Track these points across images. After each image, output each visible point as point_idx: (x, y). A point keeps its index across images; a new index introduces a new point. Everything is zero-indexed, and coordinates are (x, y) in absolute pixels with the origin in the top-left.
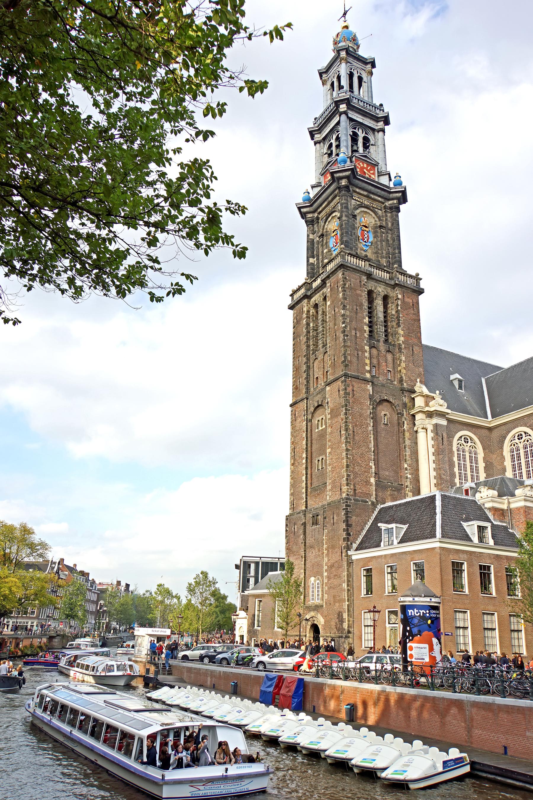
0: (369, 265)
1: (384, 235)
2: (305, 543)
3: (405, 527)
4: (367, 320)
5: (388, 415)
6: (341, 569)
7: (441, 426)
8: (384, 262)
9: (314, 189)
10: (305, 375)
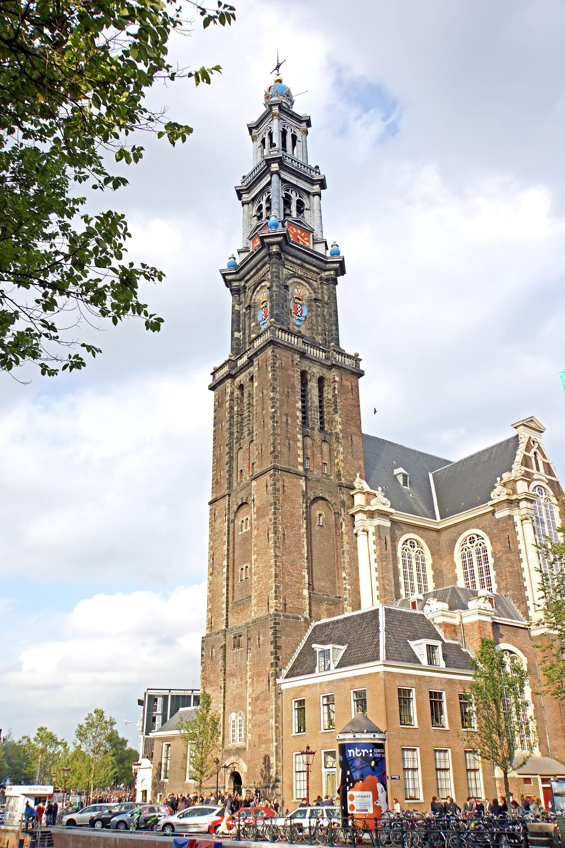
0: (303, 342)
1: (319, 309)
2: (225, 670)
3: (344, 648)
4: (299, 405)
5: (324, 515)
6: (267, 702)
7: (384, 527)
8: (319, 339)
9: (240, 254)
10: (227, 468)
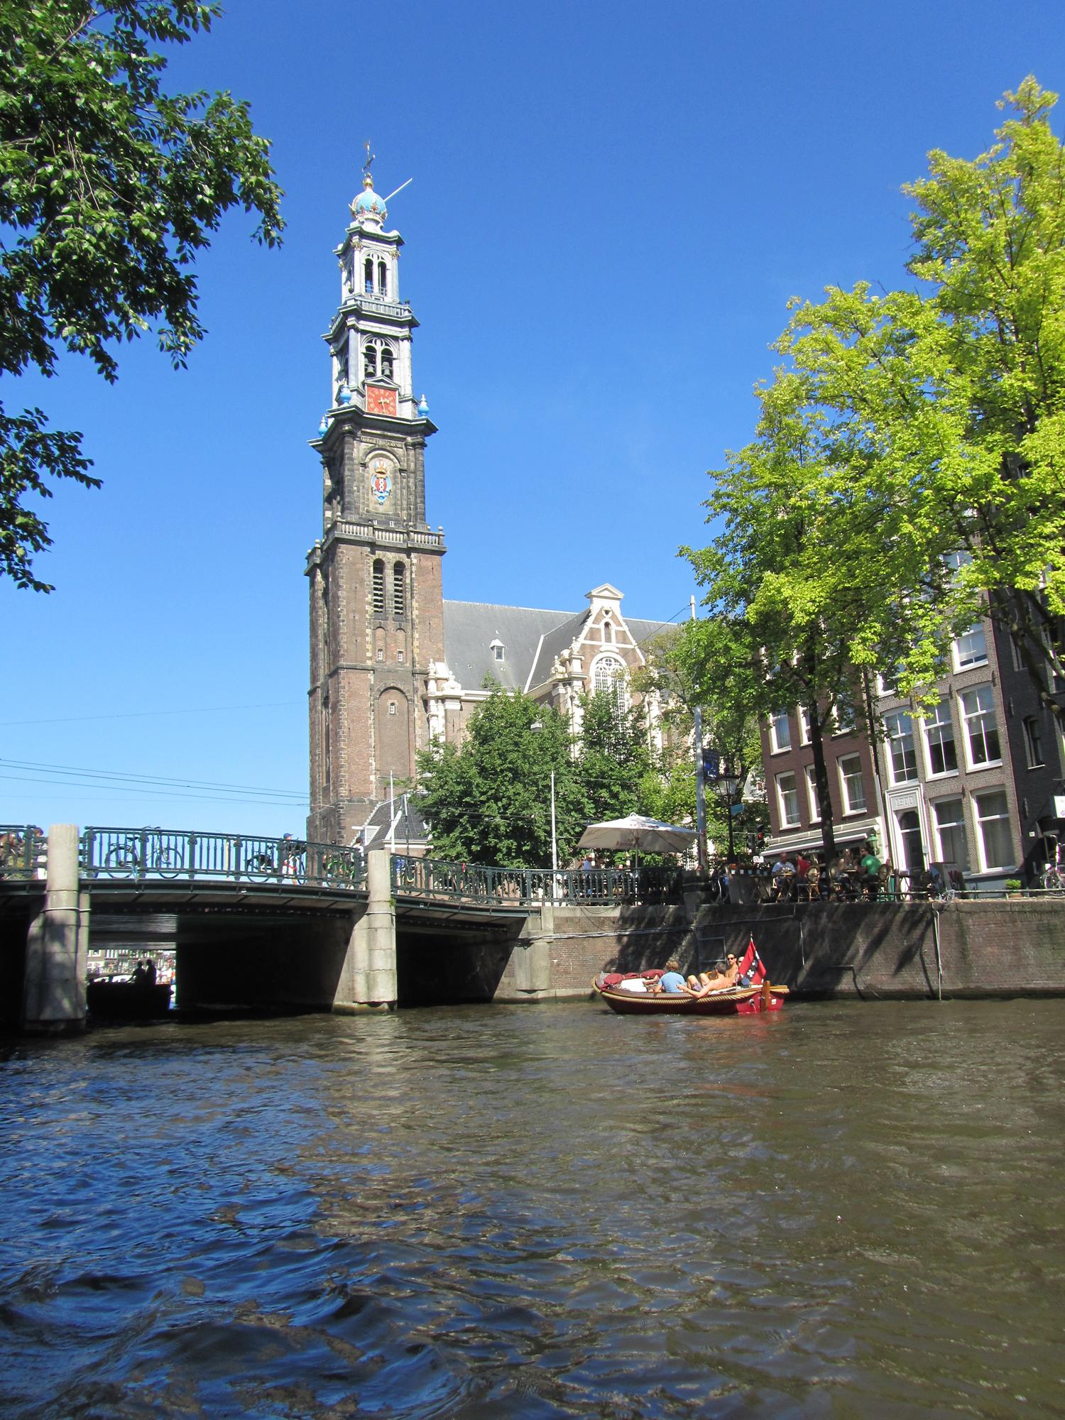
4: (370, 598)
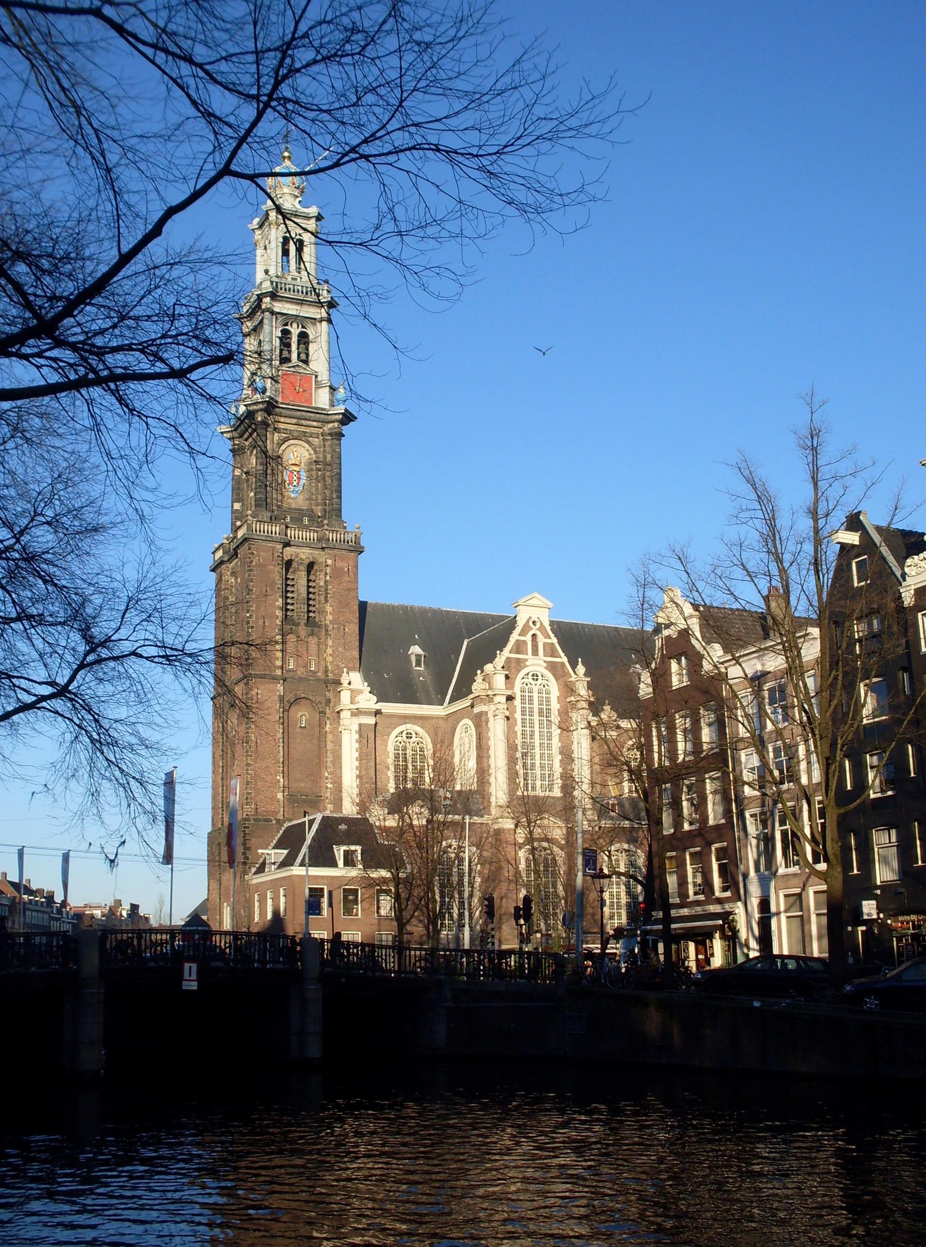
4: (280, 602)
